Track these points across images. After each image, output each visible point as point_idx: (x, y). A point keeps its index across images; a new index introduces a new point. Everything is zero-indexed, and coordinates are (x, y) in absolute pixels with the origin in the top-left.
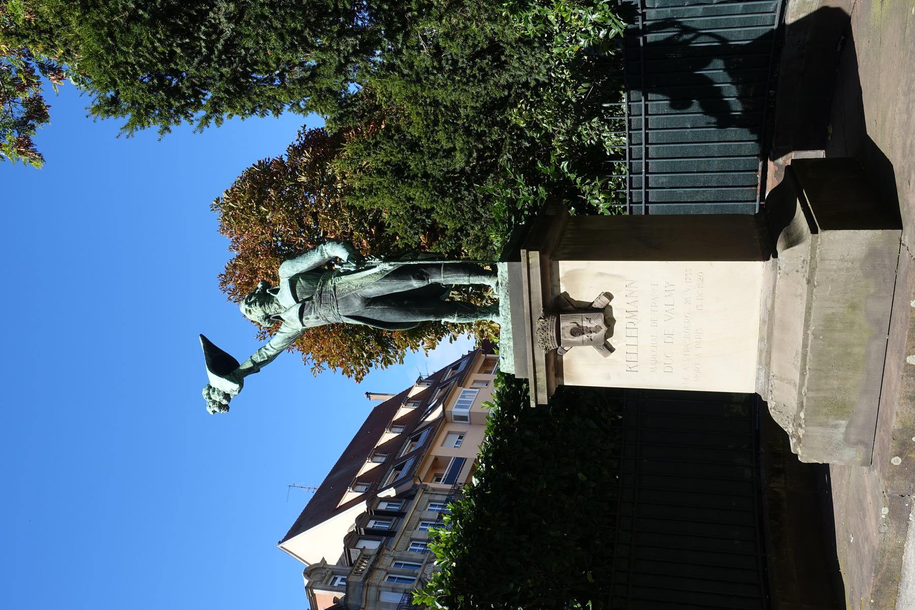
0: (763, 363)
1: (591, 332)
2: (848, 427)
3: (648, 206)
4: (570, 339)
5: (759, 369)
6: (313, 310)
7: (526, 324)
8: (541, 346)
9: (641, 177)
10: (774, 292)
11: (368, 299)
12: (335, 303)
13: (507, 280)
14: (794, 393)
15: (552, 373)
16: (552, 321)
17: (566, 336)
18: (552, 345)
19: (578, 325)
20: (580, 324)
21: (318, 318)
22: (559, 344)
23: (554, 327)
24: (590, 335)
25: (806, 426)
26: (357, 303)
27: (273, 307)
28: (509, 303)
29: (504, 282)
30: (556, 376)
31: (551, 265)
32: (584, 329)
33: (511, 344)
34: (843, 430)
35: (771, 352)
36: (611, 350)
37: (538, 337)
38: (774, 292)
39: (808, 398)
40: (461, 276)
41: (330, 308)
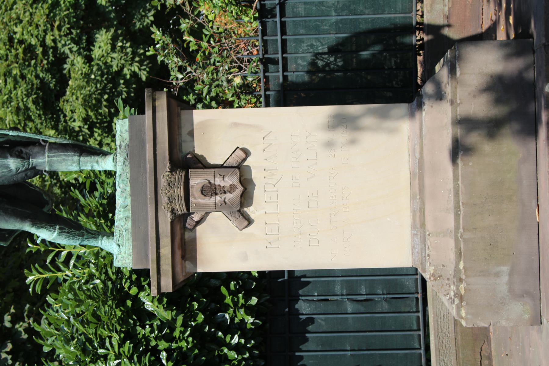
0: (418, 226)
1: (225, 193)
2: (511, 274)
5: (414, 235)
7: (149, 209)
8: (166, 207)
9: (277, 40)
13: (126, 142)
14: (452, 243)
15: (178, 254)
16: (179, 176)
17: (196, 199)
18: (180, 208)
19: (210, 183)
20: (212, 182)
23: (182, 184)
24: (224, 196)
25: (466, 276)
28: (128, 170)
29: (123, 144)
30: (183, 257)
31: (179, 115)
32: (217, 188)
33: (129, 224)
34: (505, 279)
35: (424, 209)
36: (249, 221)
37: (163, 199)
39: (465, 241)
40: (69, 156)
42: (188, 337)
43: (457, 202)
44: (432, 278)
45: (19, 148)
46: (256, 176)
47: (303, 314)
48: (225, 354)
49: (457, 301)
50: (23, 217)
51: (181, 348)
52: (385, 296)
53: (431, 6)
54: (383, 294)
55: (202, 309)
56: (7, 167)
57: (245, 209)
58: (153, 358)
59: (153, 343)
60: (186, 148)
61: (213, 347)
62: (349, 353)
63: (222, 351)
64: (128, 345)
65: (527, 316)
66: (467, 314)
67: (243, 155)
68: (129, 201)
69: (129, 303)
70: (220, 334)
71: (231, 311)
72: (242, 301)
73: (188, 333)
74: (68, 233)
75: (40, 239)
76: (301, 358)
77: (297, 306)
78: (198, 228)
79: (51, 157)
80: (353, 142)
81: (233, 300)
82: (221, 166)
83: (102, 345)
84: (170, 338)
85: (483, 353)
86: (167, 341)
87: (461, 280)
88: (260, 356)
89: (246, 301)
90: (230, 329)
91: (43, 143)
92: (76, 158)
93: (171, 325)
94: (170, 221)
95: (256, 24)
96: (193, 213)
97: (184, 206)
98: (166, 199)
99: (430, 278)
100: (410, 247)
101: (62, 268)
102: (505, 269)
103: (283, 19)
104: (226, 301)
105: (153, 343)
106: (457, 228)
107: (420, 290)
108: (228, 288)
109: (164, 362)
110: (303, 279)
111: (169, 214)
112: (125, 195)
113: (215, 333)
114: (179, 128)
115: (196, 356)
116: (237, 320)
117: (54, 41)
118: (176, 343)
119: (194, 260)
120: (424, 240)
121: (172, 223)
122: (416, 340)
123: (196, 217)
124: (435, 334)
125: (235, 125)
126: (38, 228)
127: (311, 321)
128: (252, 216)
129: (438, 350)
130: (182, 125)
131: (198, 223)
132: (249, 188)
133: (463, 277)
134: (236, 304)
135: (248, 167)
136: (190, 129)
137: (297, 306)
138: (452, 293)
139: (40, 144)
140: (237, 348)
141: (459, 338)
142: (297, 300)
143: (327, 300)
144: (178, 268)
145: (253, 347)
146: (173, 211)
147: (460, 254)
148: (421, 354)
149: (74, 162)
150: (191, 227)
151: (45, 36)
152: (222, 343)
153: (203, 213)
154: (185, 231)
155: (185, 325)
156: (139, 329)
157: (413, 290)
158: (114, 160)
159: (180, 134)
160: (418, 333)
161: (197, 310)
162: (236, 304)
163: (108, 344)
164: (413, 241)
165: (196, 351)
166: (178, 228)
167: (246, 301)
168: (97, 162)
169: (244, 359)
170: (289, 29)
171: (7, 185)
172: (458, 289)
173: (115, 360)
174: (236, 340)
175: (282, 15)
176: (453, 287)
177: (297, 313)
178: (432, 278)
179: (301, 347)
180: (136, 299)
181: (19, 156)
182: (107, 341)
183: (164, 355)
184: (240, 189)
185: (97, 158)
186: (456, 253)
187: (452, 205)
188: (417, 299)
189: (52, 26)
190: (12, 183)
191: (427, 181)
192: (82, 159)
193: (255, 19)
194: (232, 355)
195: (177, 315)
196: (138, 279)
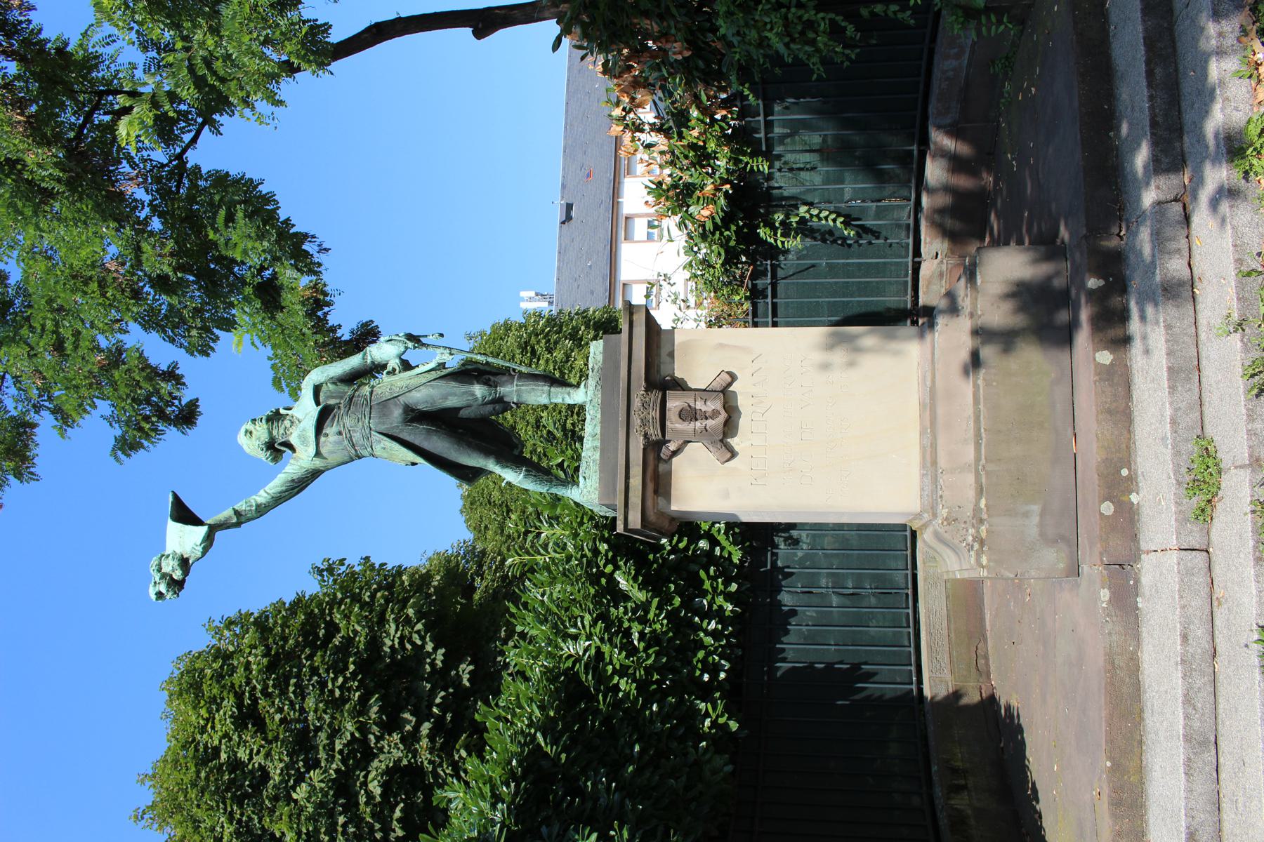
0: (929, 465)
1: (706, 418)
2: (1043, 514)
3: (776, 303)
5: (923, 475)
6: (336, 419)
11: (413, 410)
12: (368, 410)
13: (600, 364)
14: (970, 478)
15: (650, 487)
16: (656, 396)
17: (674, 424)
18: (655, 433)
19: (690, 406)
20: (693, 406)
21: (340, 433)
23: (658, 405)
24: (705, 422)
25: (989, 516)
26: (397, 413)
27: (283, 426)
28: (600, 396)
29: (596, 367)
30: (656, 492)
33: (597, 455)
34: (1035, 520)
35: (936, 444)
36: (733, 454)
37: (636, 421)
39: (987, 474)
41: (360, 416)
42: (662, 620)
43: (977, 430)
44: (945, 523)
45: (487, 377)
46: (742, 403)
47: (785, 606)
48: (701, 639)
49: (976, 546)
50: (487, 453)
51: (655, 631)
52: (873, 591)
53: (927, 287)
54: (871, 589)
55: (679, 592)
56: (473, 395)
57: (729, 440)
58: (625, 641)
59: (626, 625)
60: (664, 371)
61: (689, 632)
62: (833, 648)
63: (699, 635)
64: (600, 624)
65: (1062, 566)
66: (989, 560)
67: (729, 379)
68: (598, 430)
69: (603, 581)
70: (697, 619)
71: (709, 597)
72: (721, 587)
73: (663, 615)
74: (535, 476)
75: (505, 481)
76: (783, 650)
77: (779, 598)
78: (674, 460)
79: (520, 386)
80: (851, 364)
81: (712, 585)
82: (705, 390)
83: (575, 626)
84: (643, 621)
85: (979, 651)
86: (640, 623)
87: (981, 521)
88: (738, 645)
89: (726, 588)
90: (708, 615)
91: (513, 373)
92: (546, 388)
93: (645, 606)
94: (642, 447)
95: (747, 306)
96: (669, 441)
97: (659, 431)
98: (639, 421)
99: (942, 523)
100: (918, 489)
101: (542, 552)
102: (1036, 508)
103: (774, 300)
104: (704, 587)
105: (626, 625)
106: (978, 459)
107: (910, 585)
108: (707, 573)
109: (636, 643)
110: (786, 570)
111: (642, 438)
112: (594, 422)
113: (692, 619)
114: (659, 347)
115: (670, 640)
116: (715, 607)
117: (573, 425)
118: (650, 627)
119: (667, 496)
121: (644, 450)
122: (906, 637)
123: (672, 446)
124: (926, 630)
125: (721, 346)
126: (503, 467)
127: (793, 613)
128: (737, 448)
129: (929, 646)
130: (662, 345)
131: (675, 453)
132: (734, 416)
133: (985, 516)
134: (715, 589)
135: (734, 392)
136: (671, 350)
137: (779, 598)
138: (970, 538)
139: (510, 374)
140: (715, 634)
141: (952, 635)
142: (779, 591)
143: (811, 592)
144: (649, 503)
145: (731, 633)
146: (646, 435)
147: (982, 490)
148: (910, 652)
149: (544, 393)
150: (666, 458)
151: (566, 420)
152: (700, 628)
153: (681, 442)
154: (659, 462)
155: (660, 607)
156: (612, 610)
157: (903, 586)
159: (659, 355)
160: (907, 630)
161: (673, 592)
162: (715, 589)
163: (579, 624)
164: (922, 481)
165: (671, 634)
166: (651, 457)
167: (726, 588)
168: (569, 394)
169: (721, 646)
170: (780, 311)
171: (473, 419)
172: (978, 532)
173: (586, 641)
174: (713, 625)
175: (774, 295)
176: (972, 531)
177: (780, 604)
178: (945, 523)
179: (782, 639)
180: (611, 577)
181: (487, 383)
182: (579, 620)
183: (636, 636)
184: (723, 415)
185: (568, 389)
186: (976, 489)
187: (971, 433)
188: (907, 594)
189: (573, 413)
190: (478, 417)
191: (940, 411)
192: (552, 389)
193: (746, 298)
194: (709, 640)
195: (652, 598)
196: (614, 557)
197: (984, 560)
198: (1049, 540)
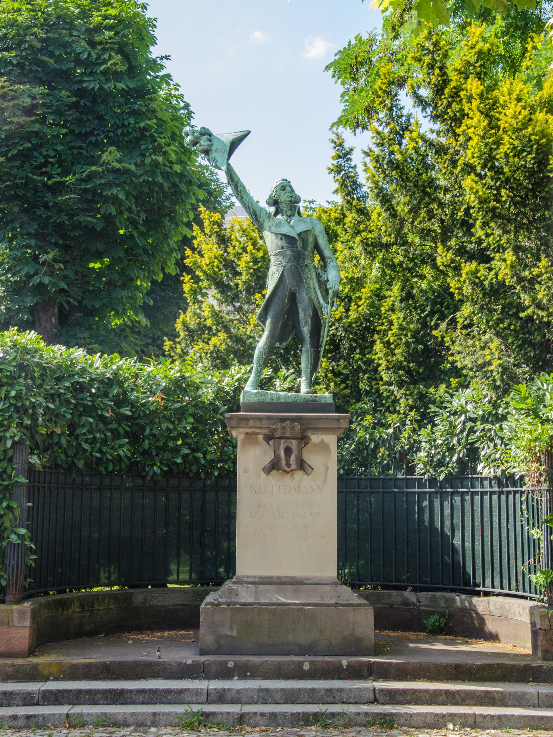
2: (231, 637)
4: (282, 446)
10: (315, 584)
21: (282, 248)
22: (277, 438)
25: (231, 609)
30: (247, 433)
31: (334, 434)
33: (268, 400)
34: (229, 633)
38: (315, 584)
66: (208, 608)
68: (282, 401)
102: (235, 633)
114: (326, 434)
120: (251, 583)
125: (327, 468)
138: (220, 600)
158: (308, 392)
191: (289, 587)
197: (209, 606)
198: (219, 637)
